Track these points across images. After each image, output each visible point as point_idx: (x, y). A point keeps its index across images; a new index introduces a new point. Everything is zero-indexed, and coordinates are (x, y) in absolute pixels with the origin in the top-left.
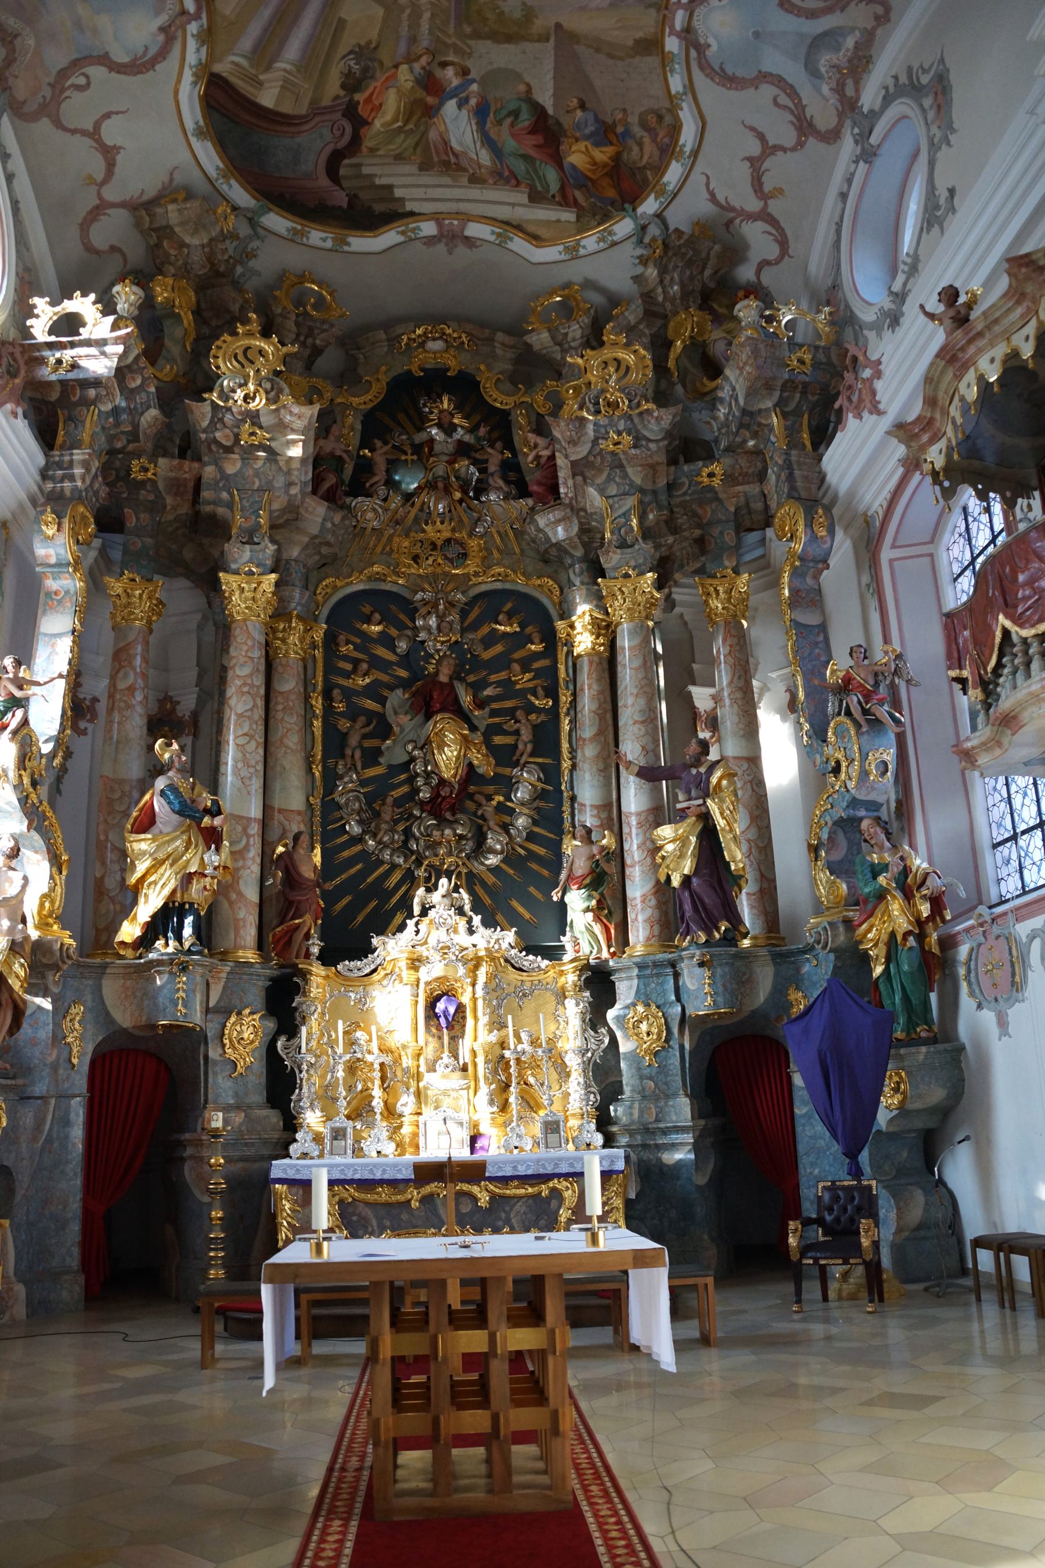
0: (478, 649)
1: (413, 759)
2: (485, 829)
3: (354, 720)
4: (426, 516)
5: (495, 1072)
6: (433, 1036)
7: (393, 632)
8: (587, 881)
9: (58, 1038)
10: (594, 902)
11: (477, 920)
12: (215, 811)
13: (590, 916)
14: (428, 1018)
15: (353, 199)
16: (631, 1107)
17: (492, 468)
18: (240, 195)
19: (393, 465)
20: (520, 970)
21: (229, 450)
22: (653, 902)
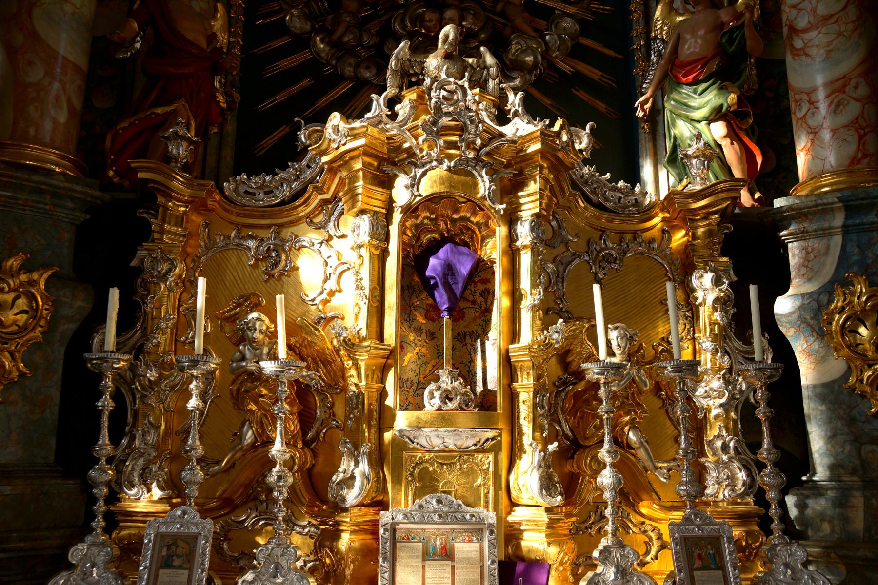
2: (508, 31)
5: (553, 418)
6: (418, 330)
8: (713, 66)
10: (732, 98)
13: (719, 130)
14: (406, 290)
16: (842, 502)
20: (600, 207)
22: (863, 90)
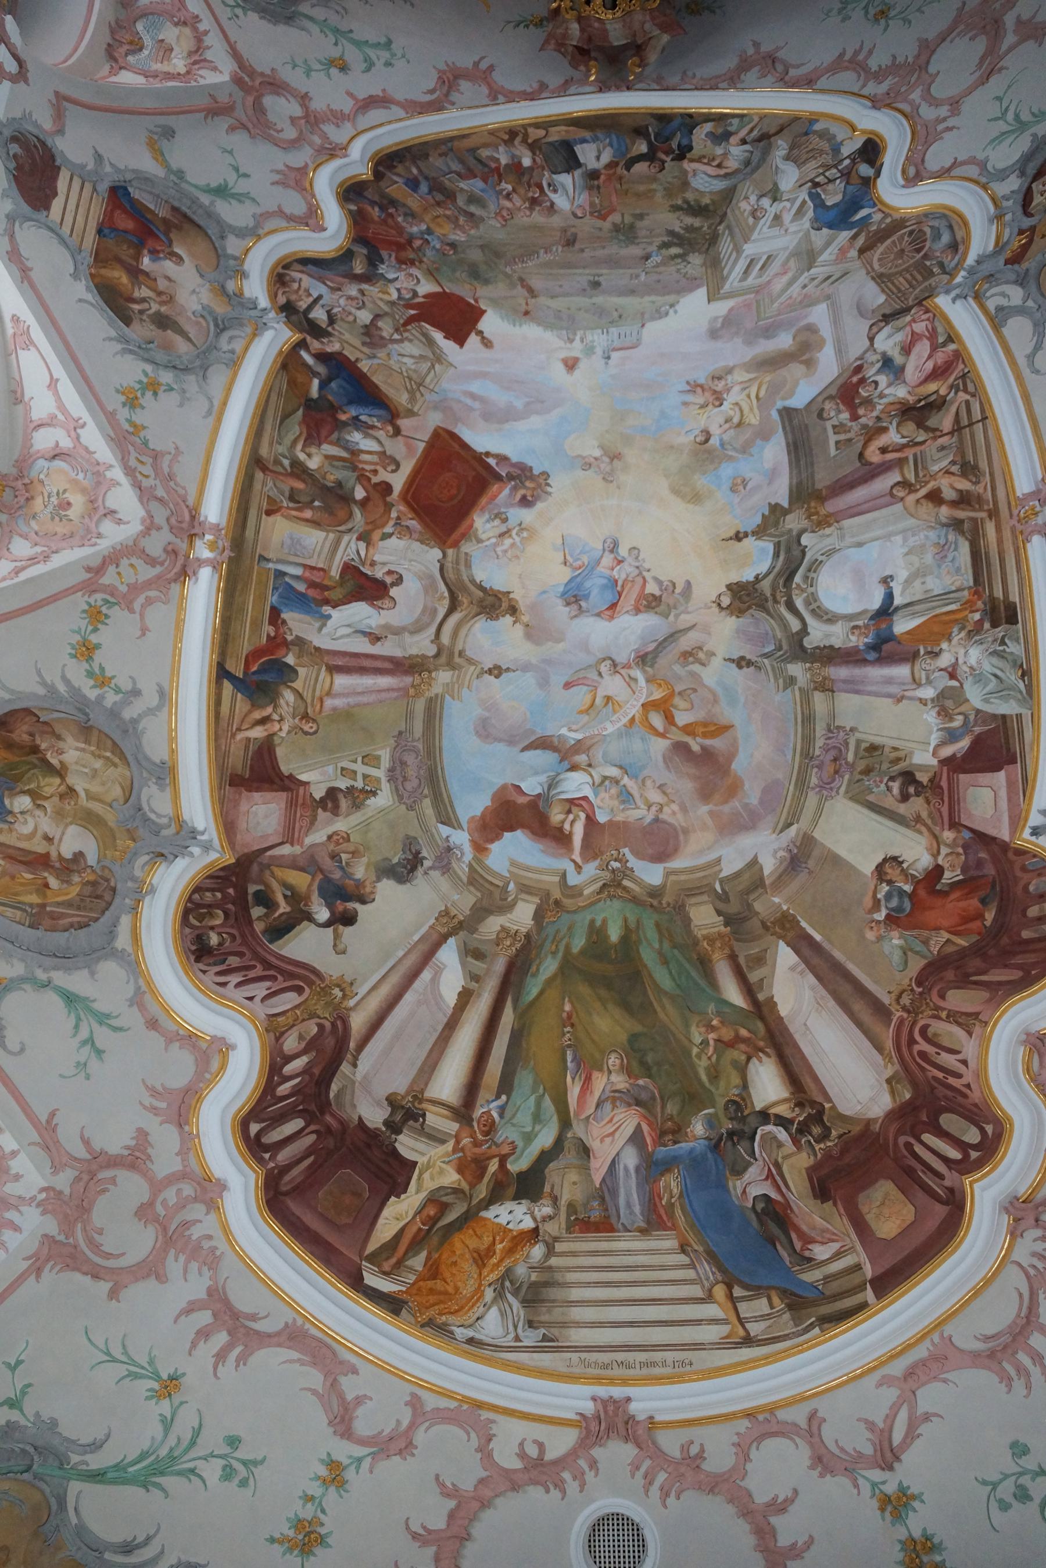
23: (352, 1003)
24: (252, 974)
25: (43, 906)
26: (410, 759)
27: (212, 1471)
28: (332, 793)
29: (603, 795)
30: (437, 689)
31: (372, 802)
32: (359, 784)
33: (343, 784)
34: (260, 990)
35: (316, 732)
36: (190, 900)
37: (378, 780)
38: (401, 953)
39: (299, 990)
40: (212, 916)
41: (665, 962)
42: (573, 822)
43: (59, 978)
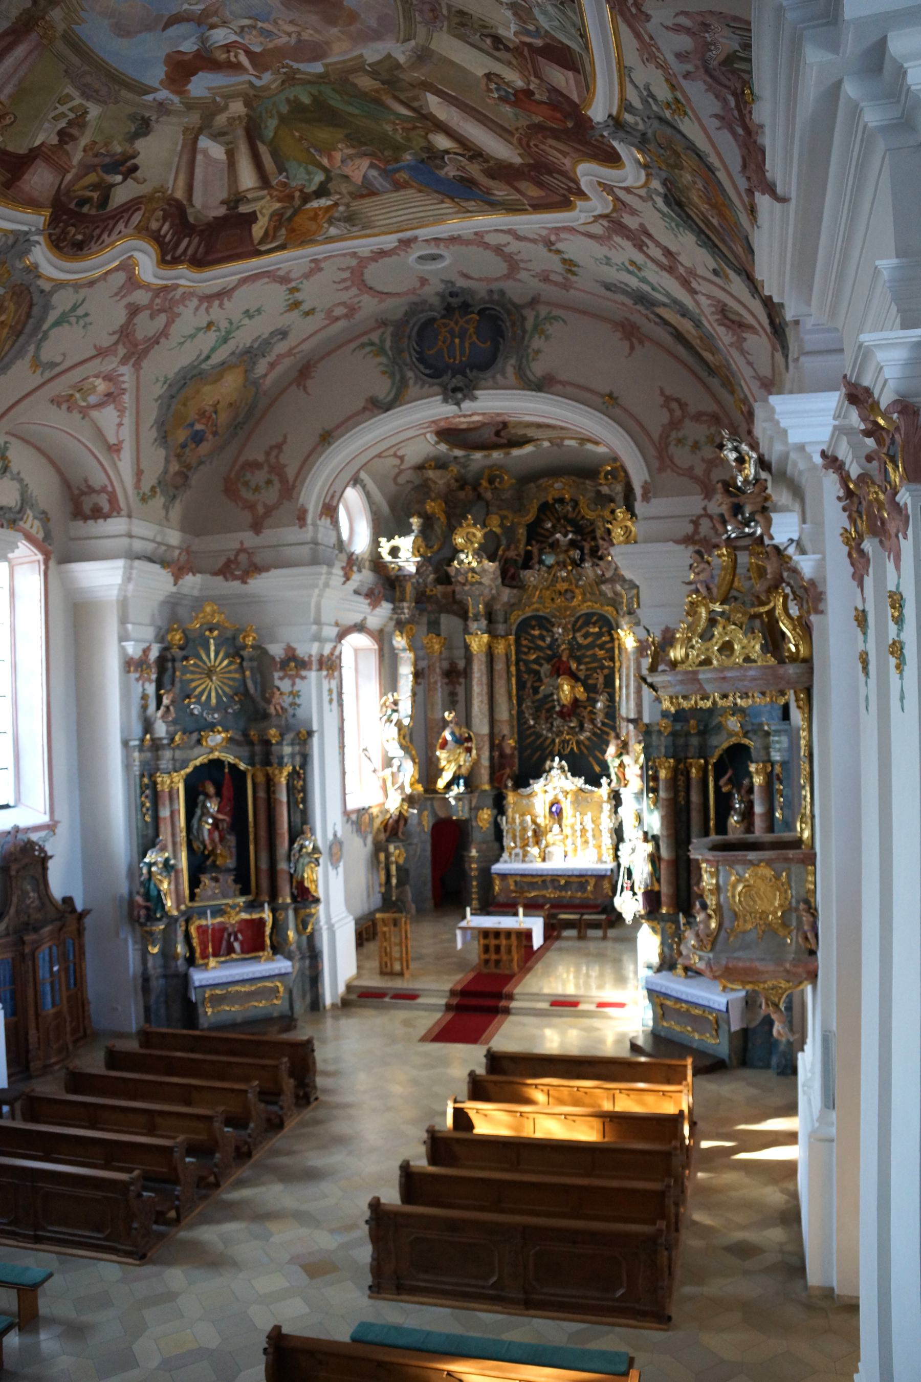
0: (580, 640)
1: (552, 694)
3: (529, 674)
4: (555, 579)
7: (545, 633)
9: (420, 823)
11: (569, 774)
12: (469, 739)
15: (509, 441)
17: (586, 551)
18: (458, 453)
19: (541, 552)
21: (464, 584)
23: (169, 192)
24: (110, 227)
25: (11, 327)
26: (88, 79)
27: (246, 321)
28: (61, 133)
29: (247, 37)
30: (61, 27)
31: (89, 117)
32: (72, 116)
33: (62, 124)
34: (121, 226)
35: (15, 117)
36: (52, 242)
37: (81, 105)
38: (176, 159)
39: (139, 209)
40: (68, 233)
41: (351, 104)
42: (236, 56)
43: (45, 327)
